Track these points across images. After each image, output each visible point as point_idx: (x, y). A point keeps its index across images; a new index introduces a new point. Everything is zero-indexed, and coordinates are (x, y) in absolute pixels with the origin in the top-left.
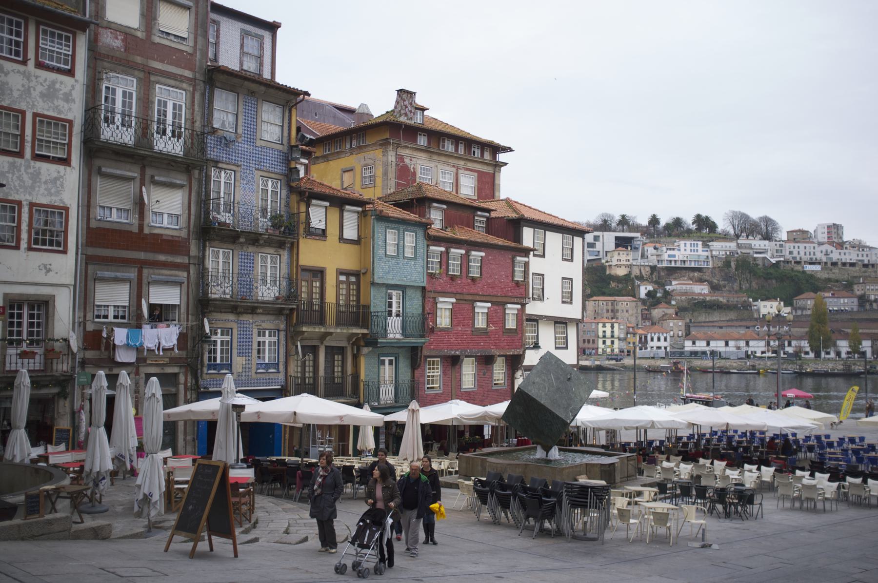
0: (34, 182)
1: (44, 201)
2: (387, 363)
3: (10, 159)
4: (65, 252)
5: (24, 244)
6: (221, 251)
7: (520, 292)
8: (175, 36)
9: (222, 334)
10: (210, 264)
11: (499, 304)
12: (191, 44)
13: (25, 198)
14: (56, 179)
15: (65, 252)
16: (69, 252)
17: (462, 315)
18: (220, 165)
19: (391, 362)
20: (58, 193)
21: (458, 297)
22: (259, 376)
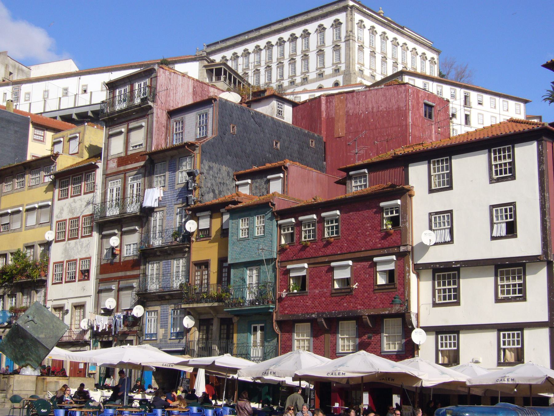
0: (81, 248)
1: (84, 256)
2: (259, 328)
3: (75, 241)
8: (139, 145)
10: (149, 272)
11: (365, 262)
12: (144, 145)
13: (78, 257)
14: (88, 244)
17: (320, 278)
18: (155, 210)
19: (262, 329)
20: (88, 250)
21: (312, 261)
22: (172, 341)
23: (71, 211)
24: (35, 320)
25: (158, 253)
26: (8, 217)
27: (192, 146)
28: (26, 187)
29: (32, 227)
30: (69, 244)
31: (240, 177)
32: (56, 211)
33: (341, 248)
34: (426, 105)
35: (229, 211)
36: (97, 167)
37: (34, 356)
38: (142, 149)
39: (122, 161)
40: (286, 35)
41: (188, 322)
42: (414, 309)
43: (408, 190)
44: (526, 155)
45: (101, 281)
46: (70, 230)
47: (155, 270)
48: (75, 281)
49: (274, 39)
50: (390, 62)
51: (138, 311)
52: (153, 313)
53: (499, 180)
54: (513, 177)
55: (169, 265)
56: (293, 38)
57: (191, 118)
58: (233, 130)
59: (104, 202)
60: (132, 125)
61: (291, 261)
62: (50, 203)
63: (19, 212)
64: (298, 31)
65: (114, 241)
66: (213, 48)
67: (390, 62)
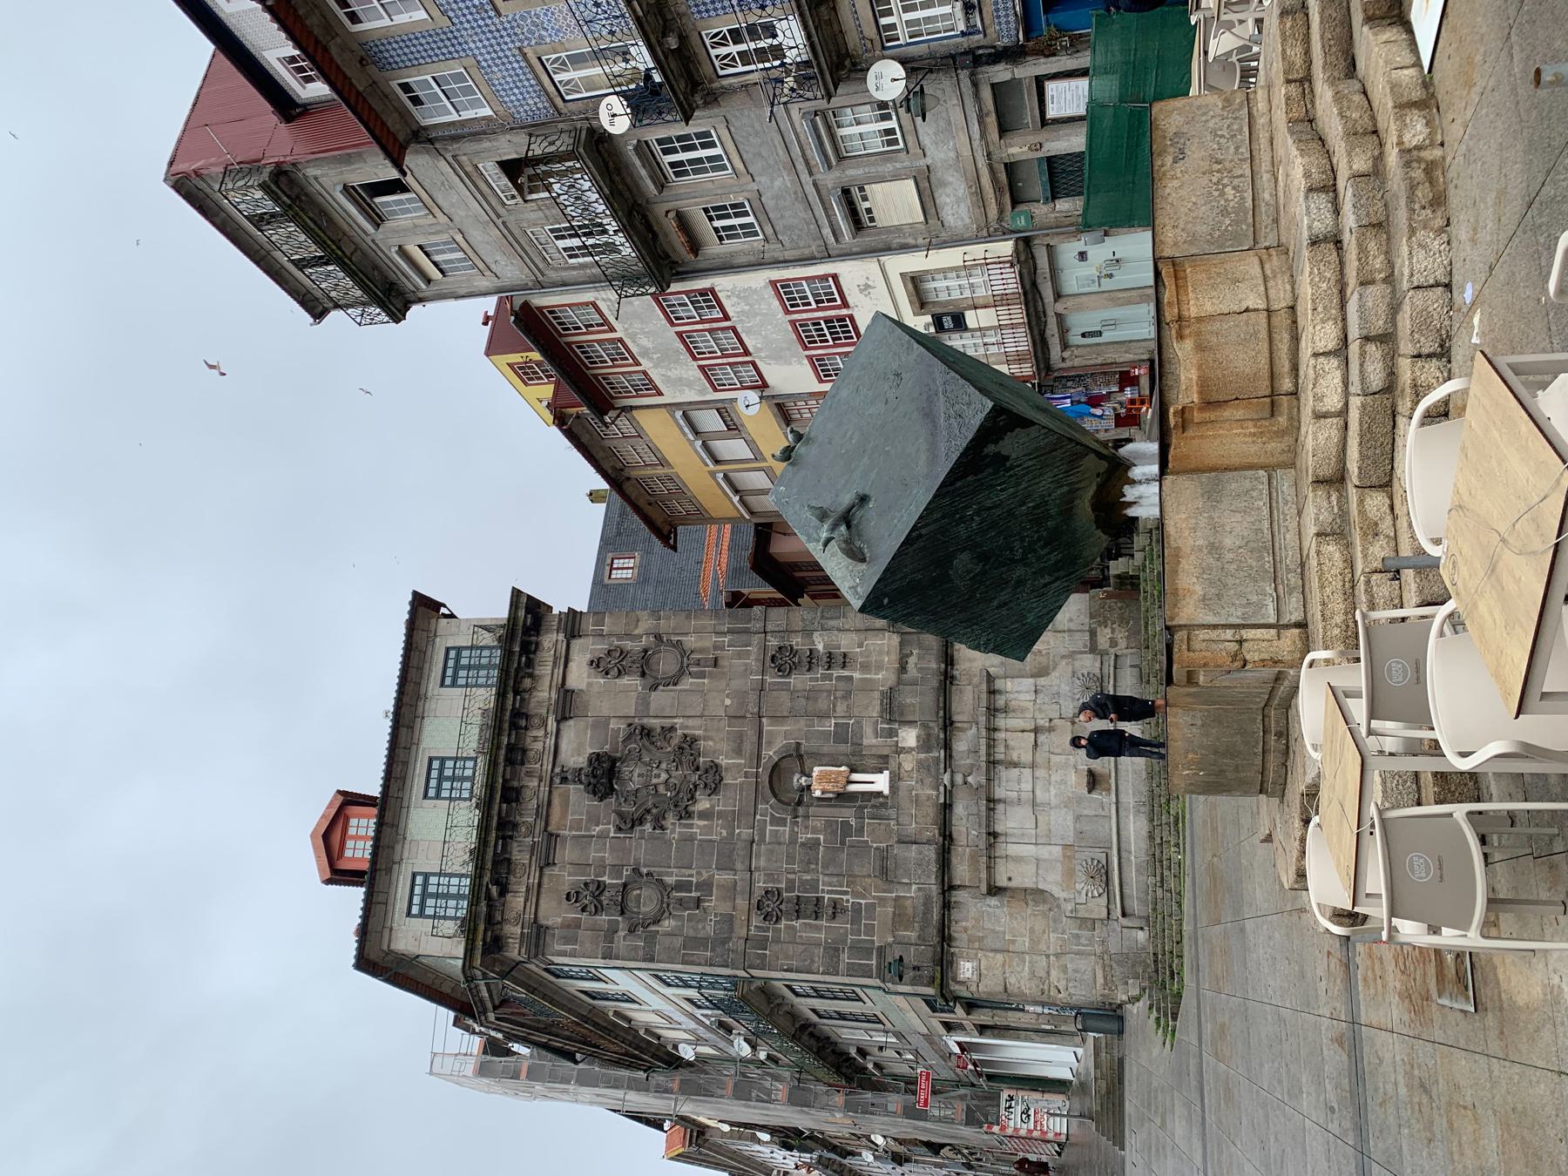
4: (835, 277)
5: (844, 312)
6: (713, 52)
9: (889, 13)
13: (782, 319)
14: (738, 297)
15: (835, 277)
16: (833, 272)
24: (847, 499)
25: (673, 43)
26: (751, 499)
28: (667, 470)
29: (751, 444)
30: (760, 350)
32: (690, 396)
36: (526, 305)
37: (1045, 483)
47: (743, 47)
48: (851, 318)
51: (887, 79)
52: (884, 21)
62: (679, 414)
63: (726, 477)
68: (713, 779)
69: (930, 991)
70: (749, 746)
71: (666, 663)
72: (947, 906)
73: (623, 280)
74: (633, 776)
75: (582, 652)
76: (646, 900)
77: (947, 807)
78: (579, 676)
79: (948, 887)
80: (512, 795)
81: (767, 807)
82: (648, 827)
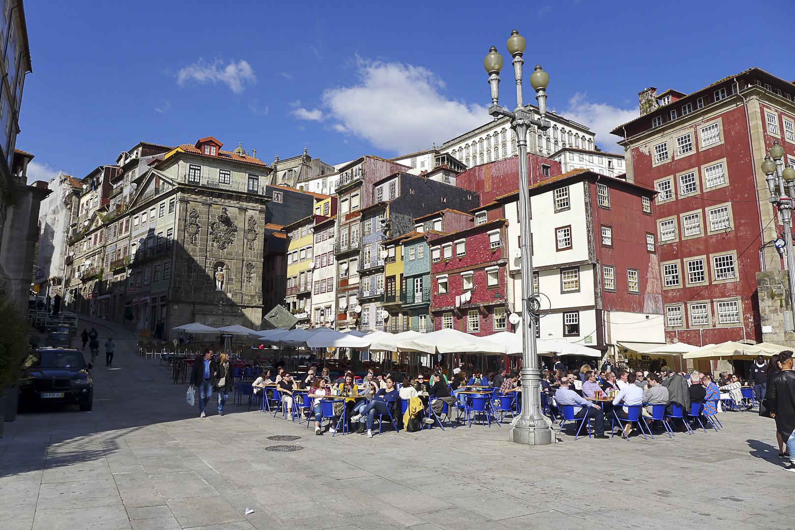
7: (498, 255)
23: (323, 250)
27: (384, 204)
31: (417, 222)
33: (466, 263)
34: (544, 167)
35: (403, 243)
38: (358, 209)
39: (348, 217)
40: (491, 133)
41: (385, 314)
42: (510, 301)
43: (504, 222)
44: (577, 191)
45: (338, 292)
46: (321, 261)
49: (484, 136)
50: (560, 144)
51: (358, 309)
53: (559, 211)
54: (569, 208)
55: (373, 278)
56: (496, 134)
57: (386, 186)
58: (412, 192)
59: (339, 244)
60: (353, 194)
61: (438, 273)
64: (499, 129)
65: (345, 266)
66: (447, 145)
67: (560, 144)
68: (223, 248)
69: (170, 298)
70: (229, 257)
71: (250, 236)
72: (190, 303)
73: (337, 247)
74: (223, 227)
75: (255, 214)
76: (192, 230)
77: (212, 304)
78: (250, 213)
79: (194, 304)
80: (220, 196)
81: (214, 261)
82: (210, 230)
